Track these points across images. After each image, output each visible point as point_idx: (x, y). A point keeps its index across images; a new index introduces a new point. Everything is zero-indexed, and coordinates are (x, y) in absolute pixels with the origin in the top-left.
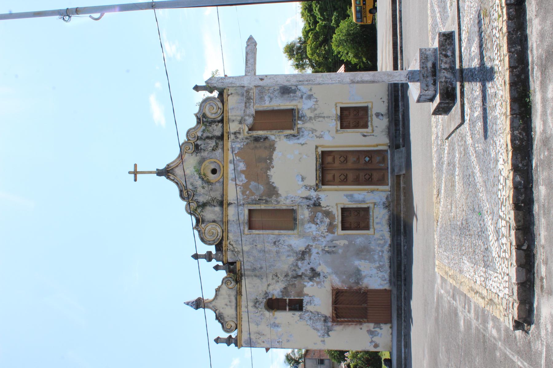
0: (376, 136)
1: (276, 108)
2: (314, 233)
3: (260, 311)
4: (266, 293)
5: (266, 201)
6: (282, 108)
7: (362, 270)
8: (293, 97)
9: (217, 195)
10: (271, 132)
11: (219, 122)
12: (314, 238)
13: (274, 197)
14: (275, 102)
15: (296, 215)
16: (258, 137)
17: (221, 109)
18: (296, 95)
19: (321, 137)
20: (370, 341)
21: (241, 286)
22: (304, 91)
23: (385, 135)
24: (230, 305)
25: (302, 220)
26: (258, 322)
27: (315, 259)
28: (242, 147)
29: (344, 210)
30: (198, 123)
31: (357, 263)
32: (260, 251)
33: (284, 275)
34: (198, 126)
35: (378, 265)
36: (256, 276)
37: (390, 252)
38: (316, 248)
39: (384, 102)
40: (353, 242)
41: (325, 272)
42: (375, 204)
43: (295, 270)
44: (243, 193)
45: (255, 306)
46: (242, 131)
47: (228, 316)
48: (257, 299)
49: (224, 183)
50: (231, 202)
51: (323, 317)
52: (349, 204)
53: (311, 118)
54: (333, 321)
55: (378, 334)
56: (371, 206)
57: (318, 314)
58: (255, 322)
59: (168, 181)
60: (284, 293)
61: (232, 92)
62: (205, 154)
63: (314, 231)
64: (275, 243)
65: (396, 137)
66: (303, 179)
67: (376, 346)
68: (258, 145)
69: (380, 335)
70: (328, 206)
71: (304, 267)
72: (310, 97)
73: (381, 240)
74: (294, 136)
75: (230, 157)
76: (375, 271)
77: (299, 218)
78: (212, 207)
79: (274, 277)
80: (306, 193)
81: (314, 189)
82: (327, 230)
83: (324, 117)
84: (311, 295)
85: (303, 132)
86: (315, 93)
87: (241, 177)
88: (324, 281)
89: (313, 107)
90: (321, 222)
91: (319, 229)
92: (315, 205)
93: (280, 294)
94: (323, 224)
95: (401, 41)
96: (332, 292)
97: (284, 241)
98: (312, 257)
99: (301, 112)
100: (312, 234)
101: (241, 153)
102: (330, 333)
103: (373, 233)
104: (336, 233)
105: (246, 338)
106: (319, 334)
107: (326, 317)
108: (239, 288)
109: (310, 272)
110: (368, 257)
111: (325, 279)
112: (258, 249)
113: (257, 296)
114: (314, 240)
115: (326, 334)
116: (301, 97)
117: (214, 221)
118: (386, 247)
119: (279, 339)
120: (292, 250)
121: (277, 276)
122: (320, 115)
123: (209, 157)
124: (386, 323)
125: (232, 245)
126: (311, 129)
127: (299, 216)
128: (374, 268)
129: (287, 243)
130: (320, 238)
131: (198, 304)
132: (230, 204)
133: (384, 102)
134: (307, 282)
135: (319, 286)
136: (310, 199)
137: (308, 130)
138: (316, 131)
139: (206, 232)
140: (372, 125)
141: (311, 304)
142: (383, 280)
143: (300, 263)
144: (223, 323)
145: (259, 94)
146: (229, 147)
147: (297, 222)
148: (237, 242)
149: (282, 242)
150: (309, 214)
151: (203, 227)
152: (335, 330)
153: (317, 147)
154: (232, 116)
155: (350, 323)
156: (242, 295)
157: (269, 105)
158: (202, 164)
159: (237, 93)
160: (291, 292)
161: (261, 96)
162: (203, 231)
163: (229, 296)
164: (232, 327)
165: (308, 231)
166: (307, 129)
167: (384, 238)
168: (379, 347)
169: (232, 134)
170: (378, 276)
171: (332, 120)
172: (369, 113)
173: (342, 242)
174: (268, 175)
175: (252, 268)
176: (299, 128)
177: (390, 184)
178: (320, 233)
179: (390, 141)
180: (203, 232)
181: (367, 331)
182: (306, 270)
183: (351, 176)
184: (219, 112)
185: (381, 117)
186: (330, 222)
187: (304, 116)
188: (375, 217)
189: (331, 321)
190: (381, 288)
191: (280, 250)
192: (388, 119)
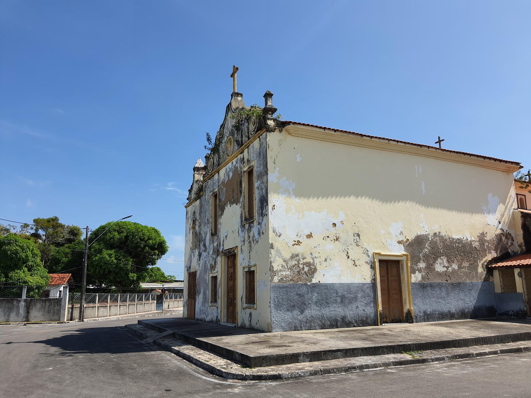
83: (250, 253)
133: (257, 324)
140: (247, 308)
146: (238, 157)
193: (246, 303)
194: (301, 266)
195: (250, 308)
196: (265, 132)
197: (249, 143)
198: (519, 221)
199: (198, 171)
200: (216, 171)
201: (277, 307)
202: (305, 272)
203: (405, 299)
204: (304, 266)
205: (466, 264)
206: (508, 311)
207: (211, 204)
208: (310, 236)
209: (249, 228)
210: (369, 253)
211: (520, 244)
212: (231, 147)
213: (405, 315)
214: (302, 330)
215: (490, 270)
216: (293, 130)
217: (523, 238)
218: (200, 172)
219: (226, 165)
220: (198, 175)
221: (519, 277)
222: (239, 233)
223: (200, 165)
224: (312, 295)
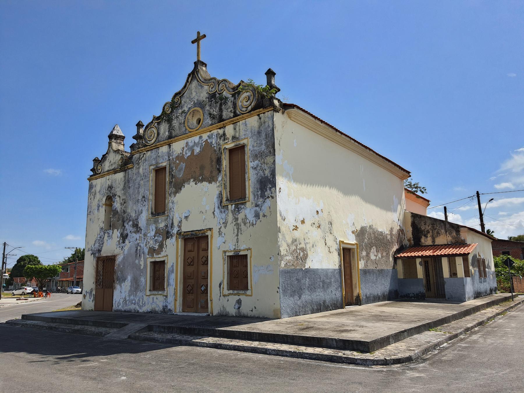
0: (219, 300)
1: (246, 176)
2: (149, 235)
3: (106, 192)
4: (115, 195)
5: (171, 182)
6: (247, 183)
8: (257, 195)
9: (176, 132)
10: (225, 175)
11: (235, 113)
14: (253, 174)
16: (220, 162)
17: (246, 111)
18: (259, 198)
19: (219, 234)
20: (87, 291)
21: (120, 172)
22: (263, 208)
25: (158, 221)
26: (101, 192)
28: (213, 146)
29: (163, 262)
30: (234, 89)
31: (129, 278)
33: (125, 209)
34: (231, 90)
35: (127, 299)
36: (125, 184)
38: (140, 237)
39: (252, 311)
42: (166, 296)
44: (178, 157)
46: (226, 141)
49: (183, 136)
50: (171, 147)
53: (237, 219)
56: (165, 294)
59: (187, 76)
61: (262, 119)
62: (208, 108)
64: (144, 197)
65: (159, 326)
66: (186, 217)
68: (214, 163)
72: (257, 216)
73: (142, 303)
74: (221, 202)
75: (205, 136)
80: (176, 224)
81: (178, 231)
82: (150, 247)
83: (237, 235)
85: (224, 212)
86: (261, 221)
87: (189, 151)
89: (248, 221)
90: (156, 241)
91: (151, 239)
92: (168, 232)
93: (115, 208)
95: (228, 347)
96: (113, 256)
97: (145, 205)
98: (134, 234)
99: (243, 206)
101: (208, 145)
102: (93, 255)
103: (147, 294)
104: (148, 256)
107: (101, 251)
108: (117, 171)
111: (121, 248)
114: (145, 235)
116: (257, 205)
117: (158, 134)
118: (138, 308)
120: (139, 215)
121: (124, 203)
122: (240, 231)
123: (205, 112)
125: (143, 157)
126: (227, 221)
127: (161, 218)
130: (145, 241)
131: (112, 137)
132: (170, 146)
133: (252, 311)
134: (120, 231)
136: (172, 227)
137: (226, 217)
138: (225, 227)
139: (152, 129)
142: (118, 304)
143: (131, 223)
145: (260, 152)
146: (212, 132)
147: (157, 217)
148: (145, 161)
150: (161, 228)
151: (155, 125)
153: (210, 229)
154: (239, 125)
156: (115, 174)
157: (249, 167)
158: (199, 107)
159: (262, 124)
161: (258, 155)
162: (152, 126)
163: (115, 163)
165: (150, 228)
166: (227, 216)
167: (143, 305)
169: (224, 132)
171: (235, 246)
172: (241, 292)
173: (142, 263)
174: (190, 180)
176: (228, 207)
177: (185, 314)
179: (215, 316)
182: (127, 230)
183: (191, 269)
184: (244, 109)
185: (237, 307)
187: (238, 211)
188: (158, 296)
190: (114, 302)
191: (139, 203)
192: (235, 315)
194: (298, 251)
195: (238, 294)
196: (272, 110)
197: (238, 120)
198: (410, 220)
199: (115, 139)
200: (166, 143)
201: (284, 292)
202: (301, 257)
203: (356, 284)
204: (301, 251)
205: (384, 254)
206: (408, 294)
207: (152, 180)
208: (303, 222)
210: (337, 240)
211: (409, 238)
212: (192, 119)
213: (354, 298)
214: (300, 315)
215: (395, 259)
216: (294, 115)
217: (412, 234)
218: (118, 141)
220: (115, 144)
221: (421, 265)
222: (214, 214)
223: (118, 133)
224: (305, 280)
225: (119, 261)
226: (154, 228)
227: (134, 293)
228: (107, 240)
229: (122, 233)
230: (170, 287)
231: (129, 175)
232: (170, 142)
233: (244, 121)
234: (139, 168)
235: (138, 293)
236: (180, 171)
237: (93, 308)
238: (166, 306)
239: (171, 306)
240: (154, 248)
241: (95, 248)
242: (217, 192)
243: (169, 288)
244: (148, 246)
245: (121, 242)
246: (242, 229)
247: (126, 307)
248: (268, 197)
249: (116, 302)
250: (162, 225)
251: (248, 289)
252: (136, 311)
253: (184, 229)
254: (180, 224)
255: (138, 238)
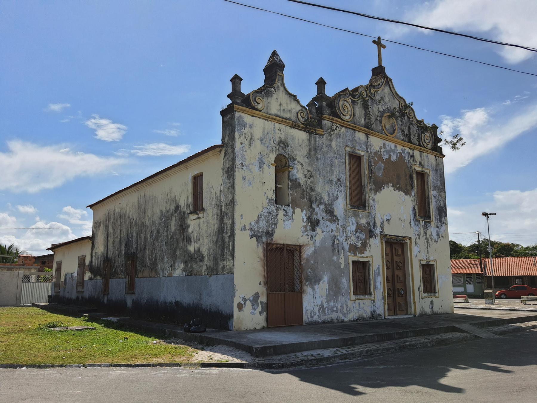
2: (348, 228)
3: (276, 147)
4: (294, 160)
7: (319, 285)
8: (437, 218)
12: (345, 227)
13: (374, 187)
15: (362, 209)
20: (246, 298)
21: (300, 130)
23: (421, 311)
24: (280, 109)
25: (359, 215)
26: (264, 141)
27: (327, 226)
31: (326, 278)
32: (331, 161)
35: (325, 307)
37: (337, 321)
38: (337, 228)
40: (343, 274)
41: (316, 238)
42: (374, 301)
43: (316, 200)
44: (375, 153)
45: (280, 142)
47: (269, 103)
48: (288, 146)
51: (272, 231)
52: (372, 270)
53: (426, 234)
54: (268, 244)
55: (255, 309)
57: (274, 224)
58: (264, 138)
60: (295, 183)
63: (350, 228)
66: (388, 220)
67: (240, 307)
68: (408, 177)
69: (253, 311)
70: (370, 246)
71: (320, 212)
72: (438, 235)
73: (347, 310)
74: (415, 216)
76: (319, 303)
77: (360, 212)
78: (364, 116)
79: (309, 172)
80: (378, 224)
83: (427, 248)
84: (294, 218)
88: (307, 235)
89: (433, 238)
90: (358, 237)
92: (370, 231)
93: (294, 178)
94: (356, 239)
96: (297, 246)
97: (341, 191)
98: (328, 223)
100: (348, 225)
102: (254, 239)
103: (352, 299)
104: (349, 254)
105: (245, 120)
106: (253, 224)
107: (272, 234)
109: (315, 219)
110: (331, 292)
111: (310, 237)
112: (334, 159)
113: (291, 147)
115: (253, 233)
118: (341, 317)
119: (246, 166)
120: (334, 200)
121: (311, 176)
124: (267, 319)
127: (361, 213)
128: (322, 301)
129: (339, 194)
133: (440, 309)
134: (306, 213)
135: (303, 229)
136: (374, 226)
140: (426, 297)
141: (285, 216)
143: (322, 207)
144: (261, 93)
147: (356, 210)
149: (340, 189)
150: (363, 224)
152: (258, 246)
153: (410, 238)
155: (266, 268)
156: (291, 127)
160: (296, 192)
163: (290, 111)
164: (257, 104)
165: (350, 221)
167: (348, 313)
168: (239, 311)
170: (314, 306)
173: (342, 261)
175: (317, 148)
178: (349, 235)
180: (346, 99)
181: (258, 292)
182: (317, 214)
185: (431, 306)
186: (357, 248)
189: (267, 241)
190: (304, 312)
193: (425, 292)
209: (425, 226)
219: (385, 140)
222: (411, 225)
225: (308, 255)
226: (354, 222)
227: (335, 298)
228: (284, 221)
229: (309, 216)
230: (377, 290)
231: (315, 141)
232: (370, 133)
233: (426, 154)
234: (331, 140)
235: (340, 297)
236: (379, 169)
237: (264, 324)
238: (375, 311)
239: (380, 310)
240: (356, 245)
241: (258, 227)
242: (412, 206)
243: (376, 292)
244: (349, 241)
245: (308, 229)
246: (430, 243)
247: (324, 317)
248: (444, 223)
249: (307, 311)
250: (364, 221)
251: (436, 293)
252: (340, 320)
253: (387, 232)
254: (382, 226)
255: (334, 229)
